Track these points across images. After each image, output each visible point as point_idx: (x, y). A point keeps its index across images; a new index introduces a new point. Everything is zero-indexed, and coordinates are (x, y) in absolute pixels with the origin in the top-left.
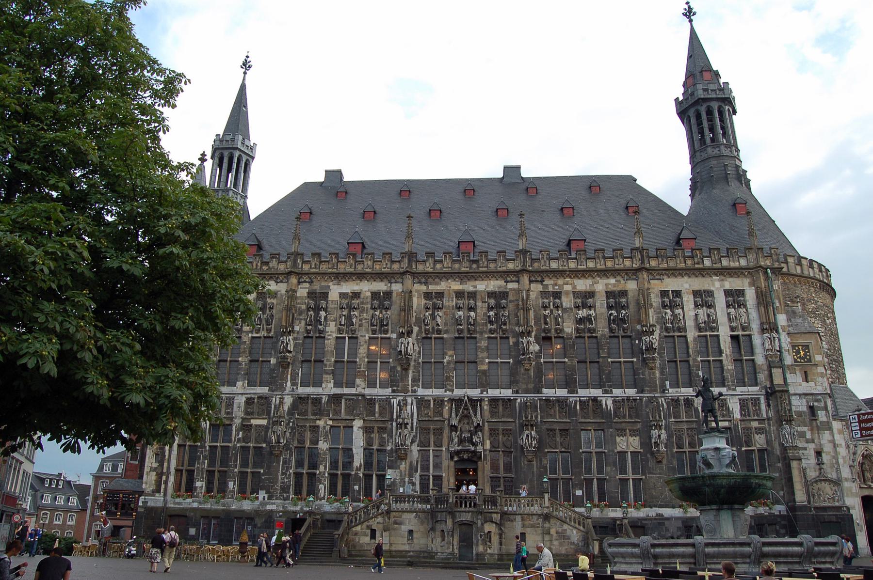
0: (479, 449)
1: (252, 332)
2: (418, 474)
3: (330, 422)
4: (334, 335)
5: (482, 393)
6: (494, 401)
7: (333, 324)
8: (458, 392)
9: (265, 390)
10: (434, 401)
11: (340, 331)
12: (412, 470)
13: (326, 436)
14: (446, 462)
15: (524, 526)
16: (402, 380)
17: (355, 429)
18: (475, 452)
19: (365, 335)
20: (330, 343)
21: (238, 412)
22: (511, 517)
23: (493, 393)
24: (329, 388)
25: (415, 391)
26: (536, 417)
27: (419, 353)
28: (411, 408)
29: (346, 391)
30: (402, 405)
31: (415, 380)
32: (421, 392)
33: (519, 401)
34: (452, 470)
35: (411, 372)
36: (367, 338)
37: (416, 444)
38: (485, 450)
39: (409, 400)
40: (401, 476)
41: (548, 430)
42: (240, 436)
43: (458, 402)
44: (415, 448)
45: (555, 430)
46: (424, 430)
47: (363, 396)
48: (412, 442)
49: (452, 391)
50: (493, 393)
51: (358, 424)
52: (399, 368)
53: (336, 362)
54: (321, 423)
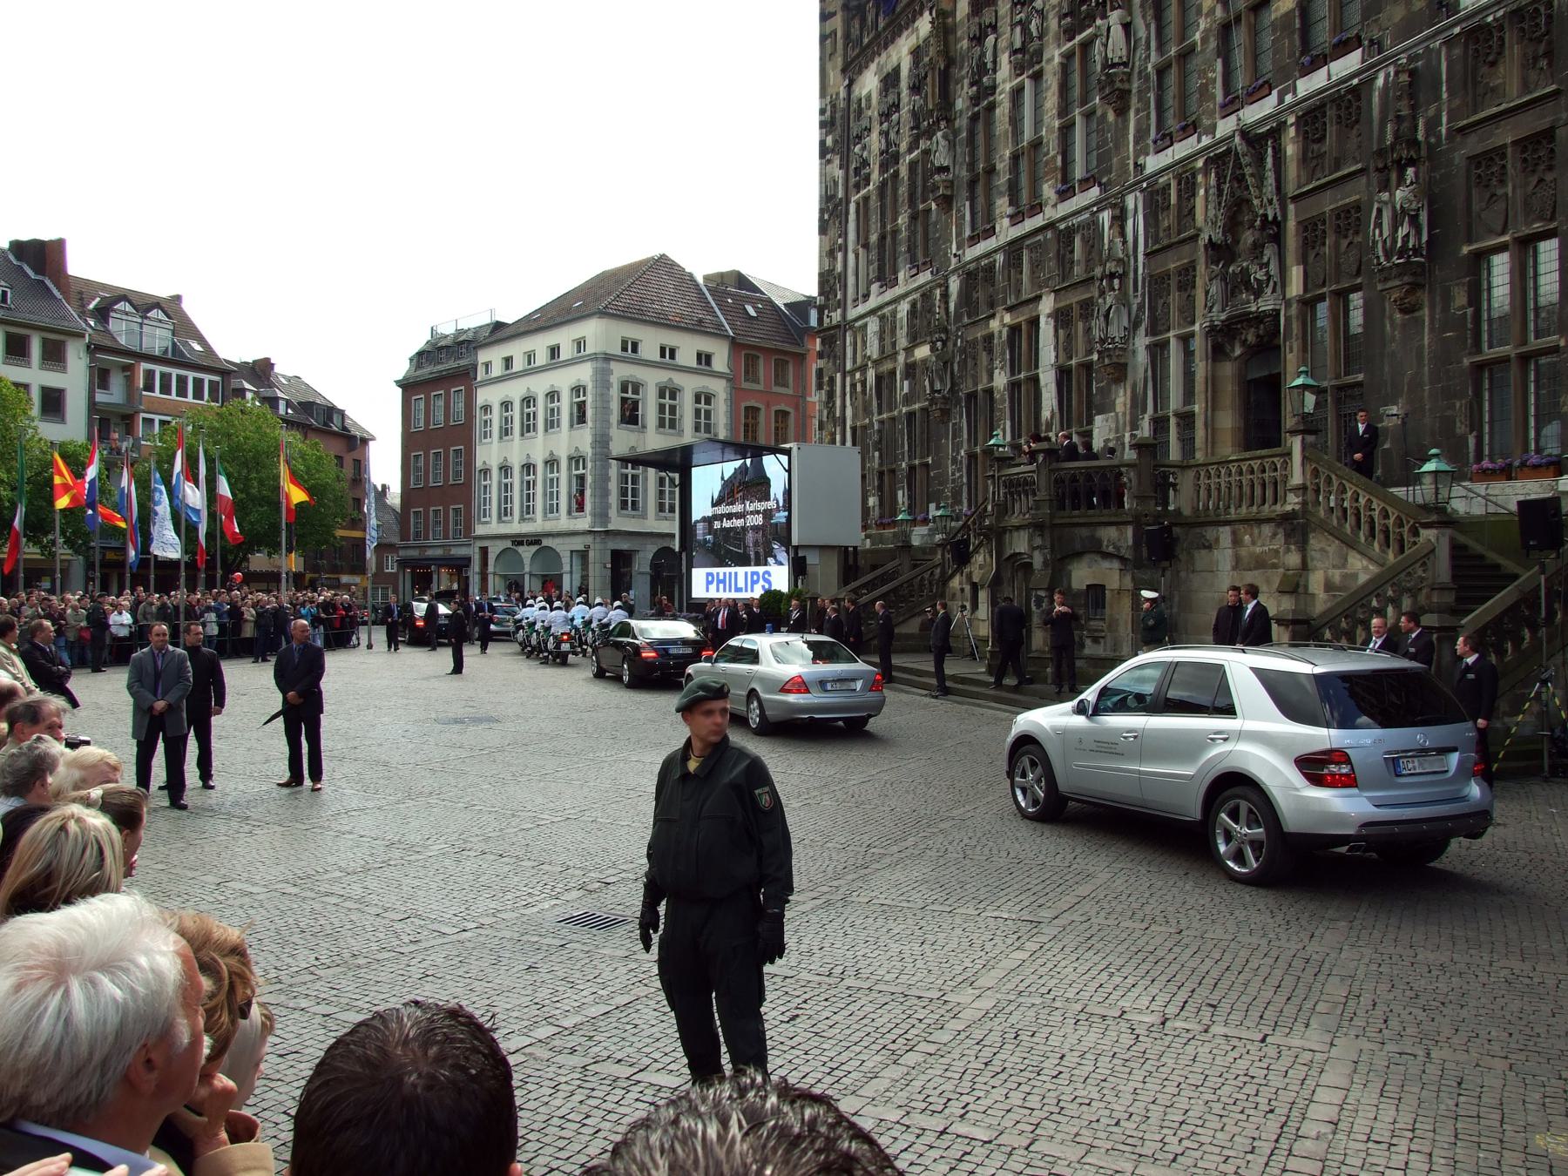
0: (1266, 304)
1: (910, 151)
2: (1147, 417)
3: (1007, 319)
4: (1008, 87)
5: (1281, 101)
6: (1312, 116)
7: (1004, 59)
8: (1226, 127)
9: (925, 277)
10: (1179, 184)
11: (1019, 69)
12: (1137, 405)
13: (1003, 353)
14: (1201, 368)
15: (1238, 564)
16: (1117, 147)
17: (1043, 320)
18: (1259, 318)
19: (1054, 55)
20: (1003, 111)
21: (903, 342)
22: (1210, 533)
23: (1310, 84)
24: (1007, 231)
25: (1139, 168)
26: (1433, 124)
27: (1148, 47)
28: (1136, 224)
29: (1030, 224)
30: (1120, 219)
31: (1141, 135)
32: (1153, 163)
33: (1380, 82)
34: (1229, 389)
35: (1132, 113)
36: (1057, 60)
37: (1142, 330)
38: (1288, 304)
39: (1130, 201)
40: (1117, 431)
41: (1475, 160)
42: (906, 390)
43: (1220, 160)
44: (1141, 341)
45: (1500, 151)
46: (1158, 283)
47: (1051, 225)
48: (1136, 325)
49: (1212, 130)
50: (1310, 84)
51: (1047, 305)
52: (1111, 117)
53: (1015, 158)
54: (994, 325)
